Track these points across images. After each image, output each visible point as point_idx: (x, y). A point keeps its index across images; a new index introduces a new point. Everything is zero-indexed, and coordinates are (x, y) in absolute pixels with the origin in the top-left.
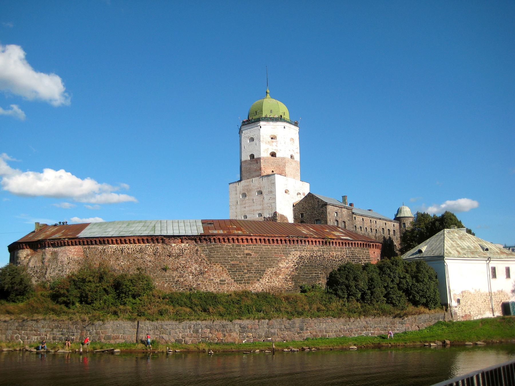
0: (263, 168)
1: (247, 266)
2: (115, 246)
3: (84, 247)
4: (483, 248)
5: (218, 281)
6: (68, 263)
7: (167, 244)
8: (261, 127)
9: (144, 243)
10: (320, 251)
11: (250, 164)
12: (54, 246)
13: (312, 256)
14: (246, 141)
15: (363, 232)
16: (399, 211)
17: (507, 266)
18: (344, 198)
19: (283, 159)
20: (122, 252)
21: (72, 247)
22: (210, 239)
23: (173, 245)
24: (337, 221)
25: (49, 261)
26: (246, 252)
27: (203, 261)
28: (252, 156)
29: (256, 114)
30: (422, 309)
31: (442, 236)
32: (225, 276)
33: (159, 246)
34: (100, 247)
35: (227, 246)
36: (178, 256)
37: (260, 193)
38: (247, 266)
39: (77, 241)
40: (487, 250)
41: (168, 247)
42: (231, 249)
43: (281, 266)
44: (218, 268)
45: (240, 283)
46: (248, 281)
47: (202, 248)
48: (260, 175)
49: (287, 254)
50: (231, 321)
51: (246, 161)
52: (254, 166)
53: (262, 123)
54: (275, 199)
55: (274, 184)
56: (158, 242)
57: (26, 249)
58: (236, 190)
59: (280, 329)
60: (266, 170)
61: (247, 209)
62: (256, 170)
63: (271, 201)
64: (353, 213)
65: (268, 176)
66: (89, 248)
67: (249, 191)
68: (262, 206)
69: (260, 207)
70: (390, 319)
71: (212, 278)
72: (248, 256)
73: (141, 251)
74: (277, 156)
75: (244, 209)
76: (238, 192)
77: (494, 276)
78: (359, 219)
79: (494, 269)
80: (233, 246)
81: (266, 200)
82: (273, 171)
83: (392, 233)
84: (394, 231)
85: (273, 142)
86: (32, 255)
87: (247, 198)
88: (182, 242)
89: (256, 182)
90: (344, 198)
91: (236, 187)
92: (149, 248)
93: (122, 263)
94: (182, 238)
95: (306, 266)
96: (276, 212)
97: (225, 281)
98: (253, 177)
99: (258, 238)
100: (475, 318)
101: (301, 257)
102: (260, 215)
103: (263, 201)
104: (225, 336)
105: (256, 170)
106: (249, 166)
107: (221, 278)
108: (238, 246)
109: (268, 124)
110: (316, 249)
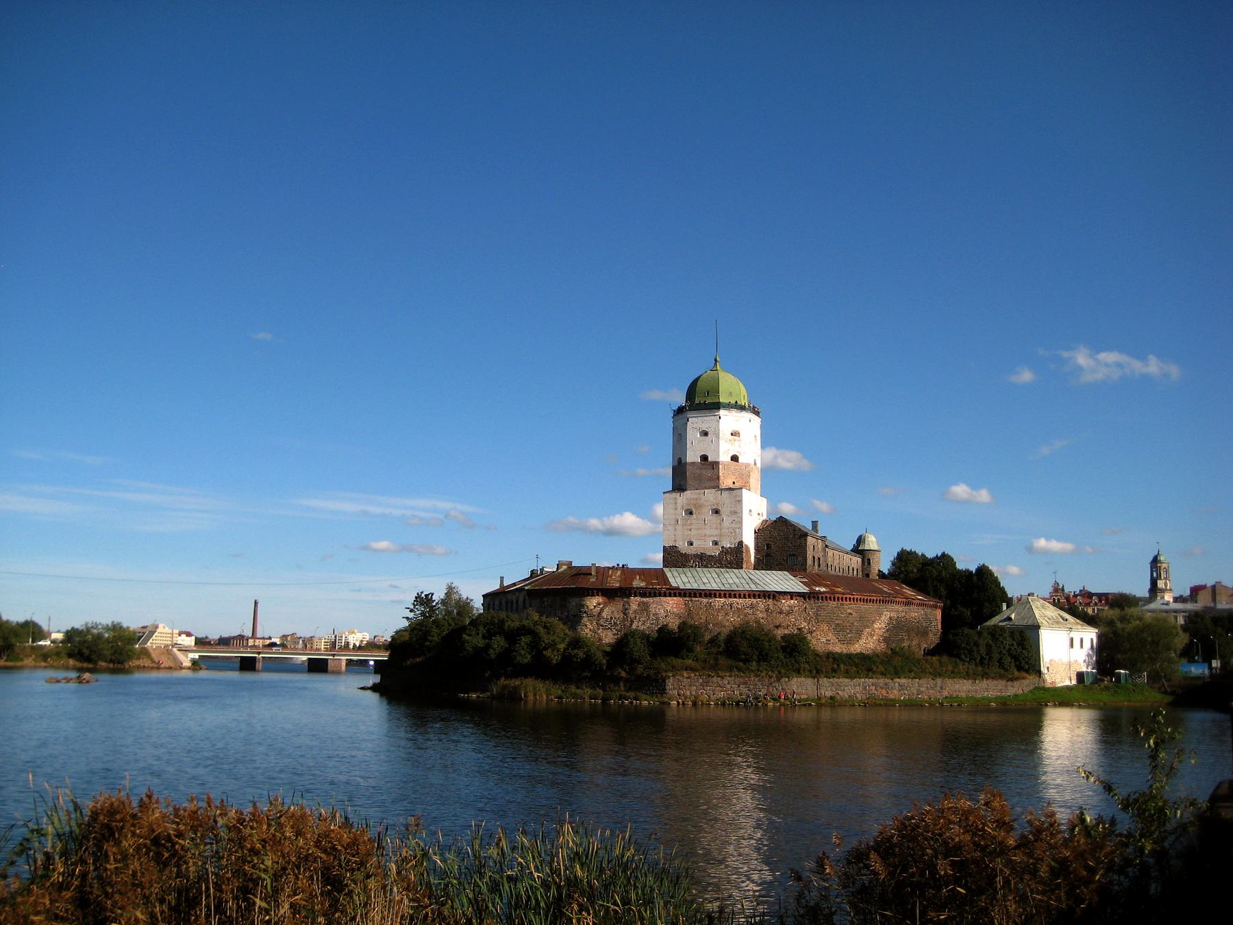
0: (721, 478)
1: (850, 626)
2: (723, 600)
3: (685, 599)
4: (1063, 619)
5: (825, 641)
6: (666, 616)
7: (777, 601)
8: (720, 418)
9: (755, 598)
10: (903, 612)
11: (701, 468)
12: (643, 595)
13: (898, 617)
14: (692, 435)
15: (833, 572)
16: (860, 540)
17: (1082, 637)
18: (815, 524)
19: (747, 465)
20: (731, 608)
21: (669, 598)
22: (818, 597)
23: (783, 601)
24: (814, 557)
25: (635, 611)
26: (849, 611)
27: (812, 619)
28: (704, 458)
29: (708, 394)
30: (1024, 674)
31: (1028, 605)
32: (831, 636)
33: (770, 602)
34: (705, 600)
35: (833, 604)
36: (789, 613)
37: (717, 512)
38: (850, 626)
39: (677, 592)
40: (1066, 620)
41: (779, 604)
42: (836, 607)
43: (875, 626)
44: (825, 627)
45: (844, 643)
46: (850, 642)
47: (810, 605)
48: (717, 487)
49: (880, 615)
50: (892, 680)
51: (694, 463)
52: (709, 473)
53: (722, 412)
54: (741, 522)
55: (740, 501)
56: (769, 598)
57: (597, 597)
58: (676, 503)
59: (927, 687)
60: (726, 481)
61: (694, 532)
62: (710, 479)
63: (733, 525)
64: (826, 546)
65: (730, 489)
66: (691, 601)
67: (699, 506)
68: (718, 530)
69: (716, 532)
70: (1003, 682)
71: (819, 637)
72: (851, 616)
73: (752, 607)
74: (740, 460)
75: (689, 532)
76: (679, 506)
77: (1072, 646)
78: (830, 553)
79: (1072, 640)
80: (837, 604)
81: (726, 523)
82: (734, 483)
83: (837, 569)
84: (857, 570)
85: (735, 440)
86: (605, 605)
87: (694, 516)
88: (792, 599)
89: (710, 496)
90: (815, 524)
91: (676, 498)
92: (761, 604)
93: (732, 619)
94: (792, 595)
95: (895, 628)
96: (742, 541)
97: (830, 640)
98: (706, 488)
99: (859, 597)
100: (1059, 685)
101: (890, 618)
102: (716, 543)
103: (720, 524)
104: (888, 693)
105: (710, 479)
106: (698, 471)
107: (828, 638)
108: (841, 604)
109: (729, 414)
110: (901, 609)
